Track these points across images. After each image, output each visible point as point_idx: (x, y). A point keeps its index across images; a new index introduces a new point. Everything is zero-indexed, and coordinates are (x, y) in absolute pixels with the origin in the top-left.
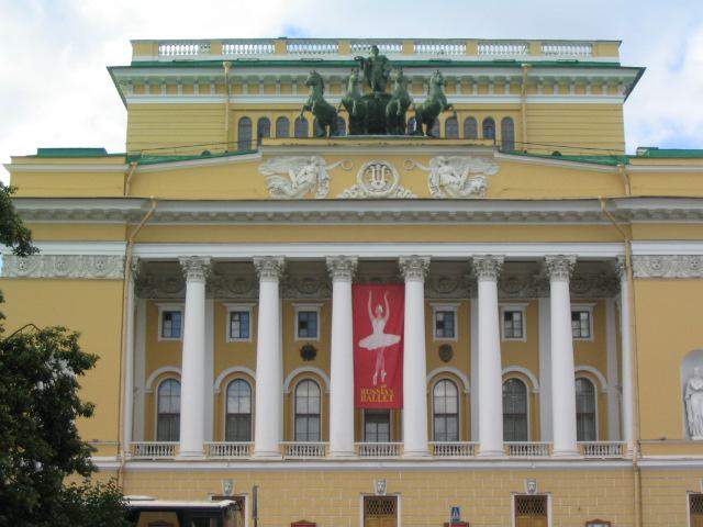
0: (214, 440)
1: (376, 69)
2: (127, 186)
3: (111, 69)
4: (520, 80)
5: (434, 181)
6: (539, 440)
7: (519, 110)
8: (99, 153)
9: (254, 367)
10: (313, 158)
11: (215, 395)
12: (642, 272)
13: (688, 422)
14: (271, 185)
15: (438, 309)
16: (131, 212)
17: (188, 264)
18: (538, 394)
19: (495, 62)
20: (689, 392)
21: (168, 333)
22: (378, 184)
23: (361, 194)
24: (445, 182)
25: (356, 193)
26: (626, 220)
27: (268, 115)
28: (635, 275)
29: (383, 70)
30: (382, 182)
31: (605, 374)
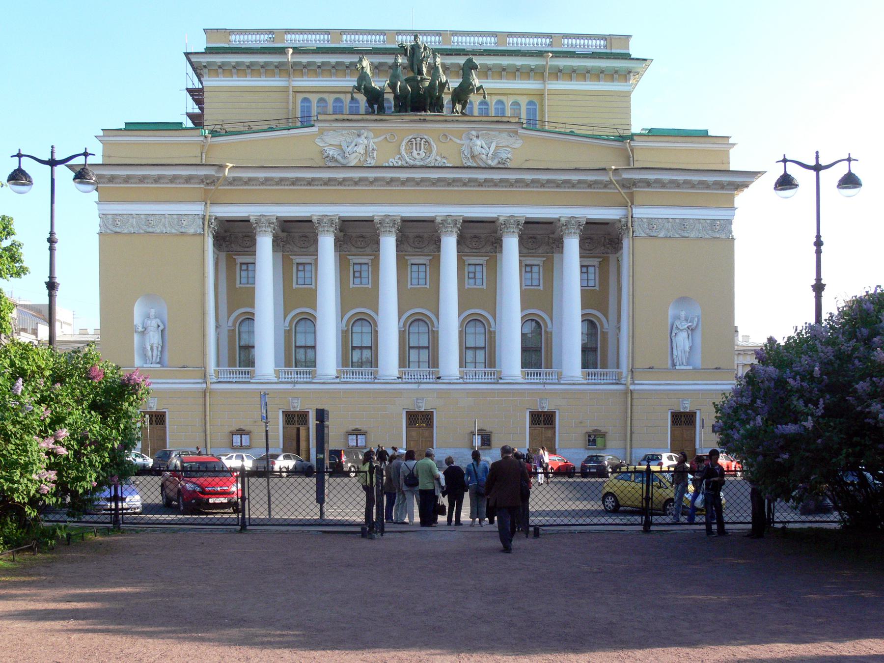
0: (285, 367)
2: (204, 155)
6: (552, 368)
14: (326, 155)
15: (470, 262)
16: (207, 177)
17: (258, 222)
20: (675, 331)
21: (244, 281)
22: (418, 154)
30: (422, 153)
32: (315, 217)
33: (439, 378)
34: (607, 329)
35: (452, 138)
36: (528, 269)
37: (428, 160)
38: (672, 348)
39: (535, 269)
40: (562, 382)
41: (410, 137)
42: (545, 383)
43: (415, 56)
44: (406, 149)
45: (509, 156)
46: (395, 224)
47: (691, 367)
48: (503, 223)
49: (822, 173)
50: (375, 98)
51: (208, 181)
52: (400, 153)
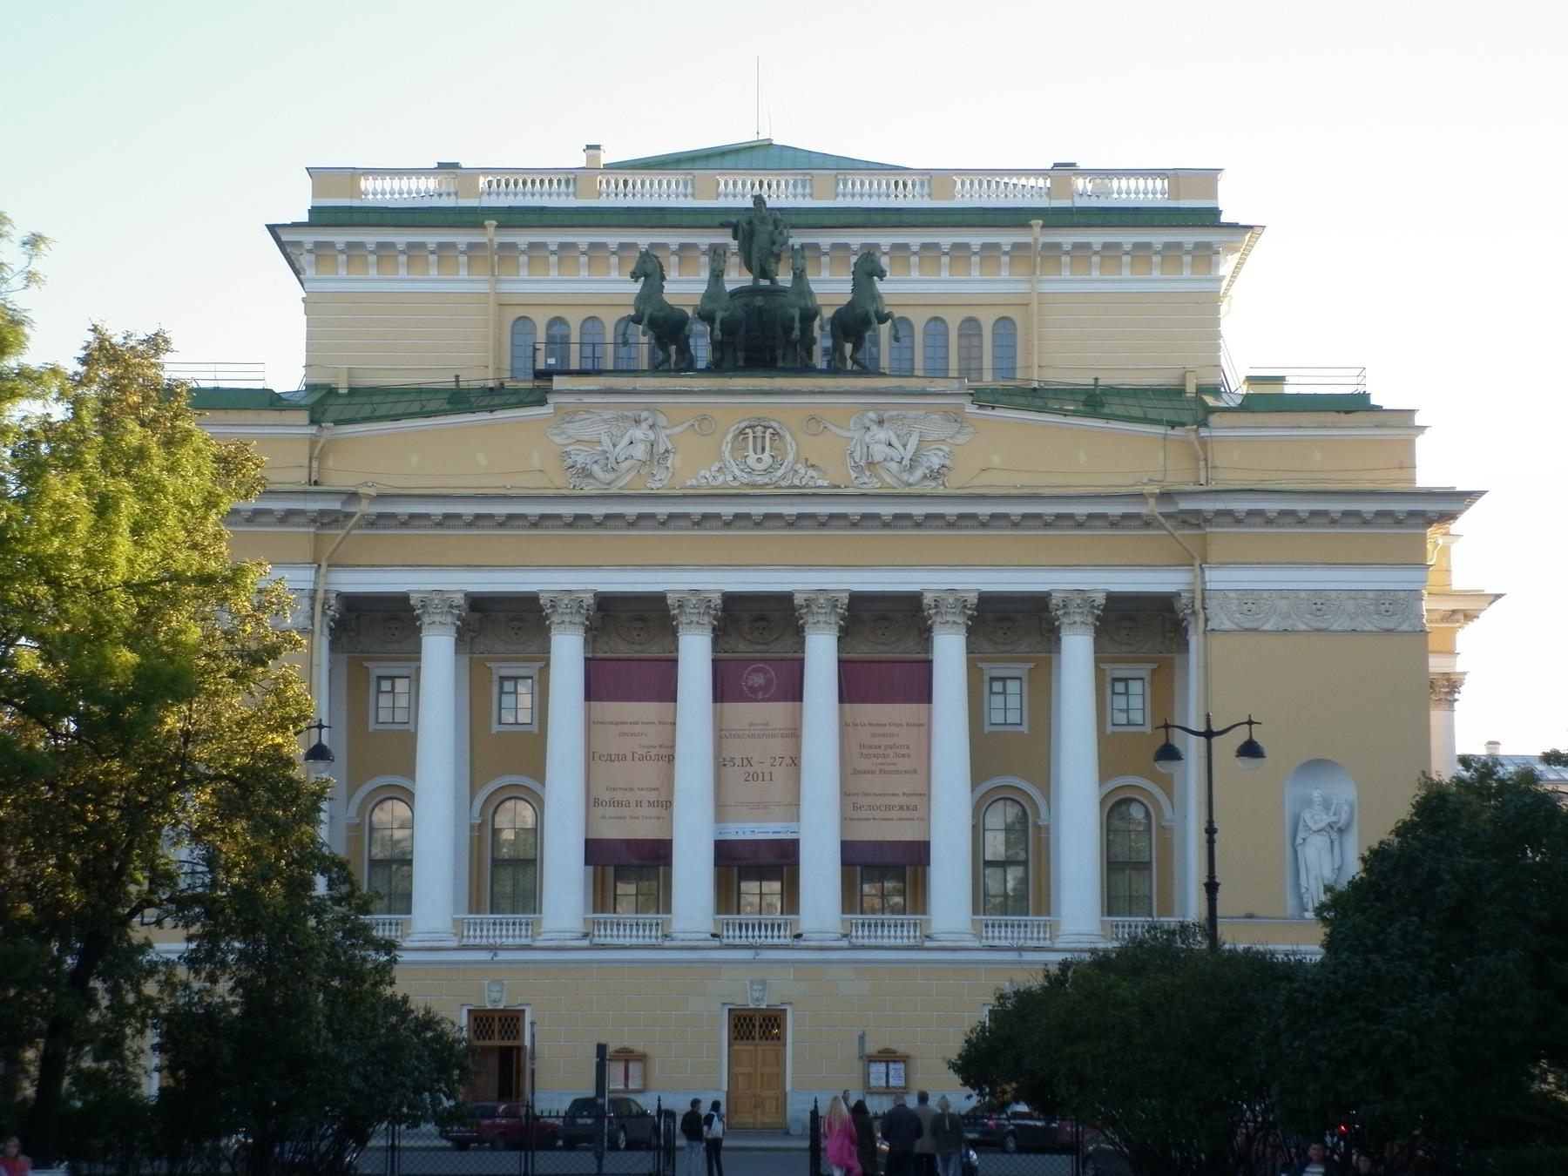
1: (762, 238)
2: (315, 464)
3: (273, 229)
5: (857, 456)
8: (268, 401)
11: (472, 826)
12: (1221, 621)
13: (1297, 885)
14: (570, 462)
16: (323, 513)
18: (1048, 829)
20: (1301, 834)
22: (759, 460)
23: (730, 478)
25: (721, 478)
26: (1198, 526)
28: (1210, 625)
29: (774, 243)
30: (766, 456)
32: (546, 595)
34: (1171, 821)
35: (828, 425)
37: (780, 473)
38: (1297, 870)
39: (1013, 687)
40: (1058, 946)
41: (743, 425)
42: (1020, 949)
43: (755, 240)
44: (732, 449)
45: (947, 462)
46: (709, 607)
48: (933, 604)
49: (1215, 740)
51: (325, 521)
52: (721, 459)
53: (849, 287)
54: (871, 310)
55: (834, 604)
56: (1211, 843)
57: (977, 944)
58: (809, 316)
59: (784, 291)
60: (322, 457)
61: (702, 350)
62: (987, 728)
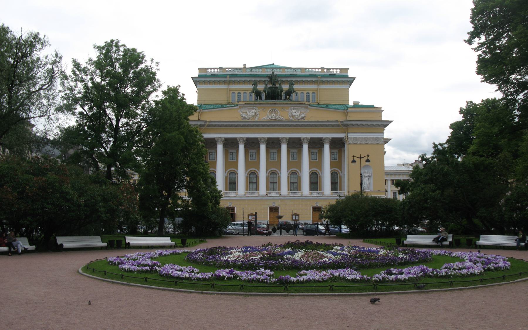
1: (273, 78)
3: (192, 78)
4: (317, 81)
7: (317, 90)
9: (237, 168)
10: (254, 108)
11: (225, 177)
12: (351, 142)
15: (292, 151)
17: (218, 139)
19: (310, 75)
24: (293, 115)
25: (267, 118)
26: (347, 126)
27: (240, 91)
29: (275, 79)
30: (275, 115)
31: (341, 171)
33: (281, 195)
36: (313, 153)
39: (315, 153)
47: (369, 190)
49: (362, 159)
50: (258, 94)
52: (267, 115)
53: (288, 87)
54: (292, 90)
55: (286, 139)
56: (361, 176)
57: (310, 196)
58: (282, 91)
59: (277, 88)
60: (200, 115)
61: (263, 97)
62: (311, 160)
